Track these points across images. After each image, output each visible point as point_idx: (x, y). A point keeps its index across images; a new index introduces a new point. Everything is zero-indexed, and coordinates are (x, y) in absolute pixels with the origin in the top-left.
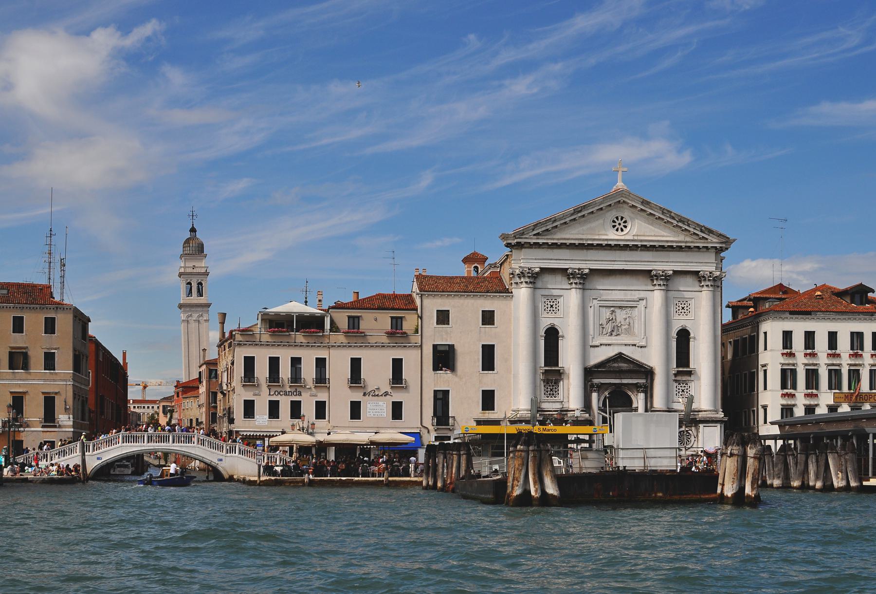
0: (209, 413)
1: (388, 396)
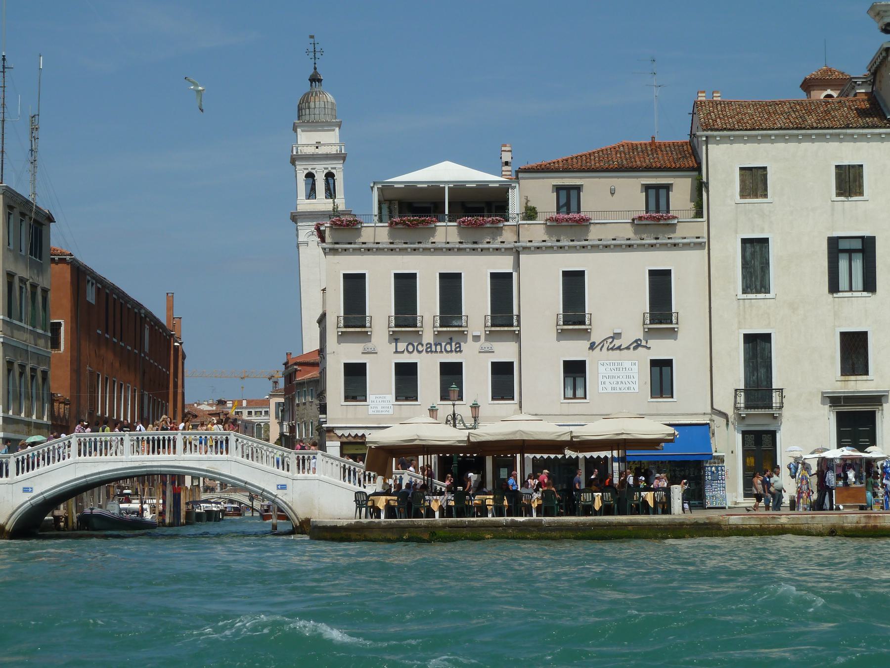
1: (640, 348)
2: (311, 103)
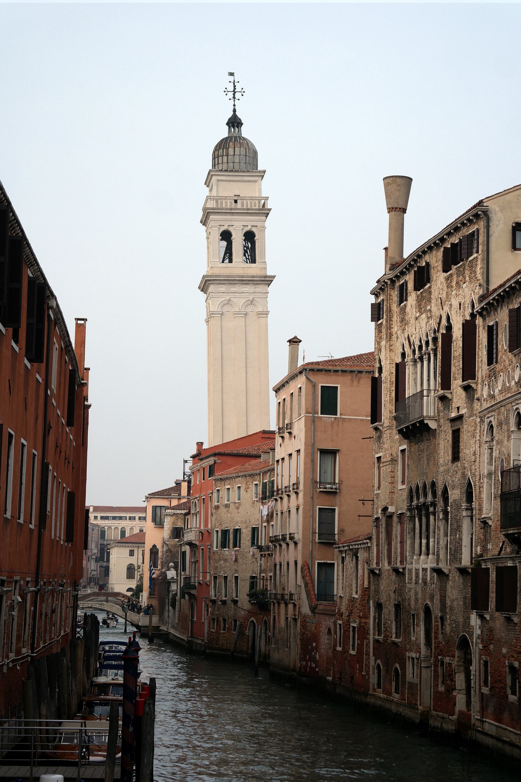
0: (314, 511)
2: (230, 149)
